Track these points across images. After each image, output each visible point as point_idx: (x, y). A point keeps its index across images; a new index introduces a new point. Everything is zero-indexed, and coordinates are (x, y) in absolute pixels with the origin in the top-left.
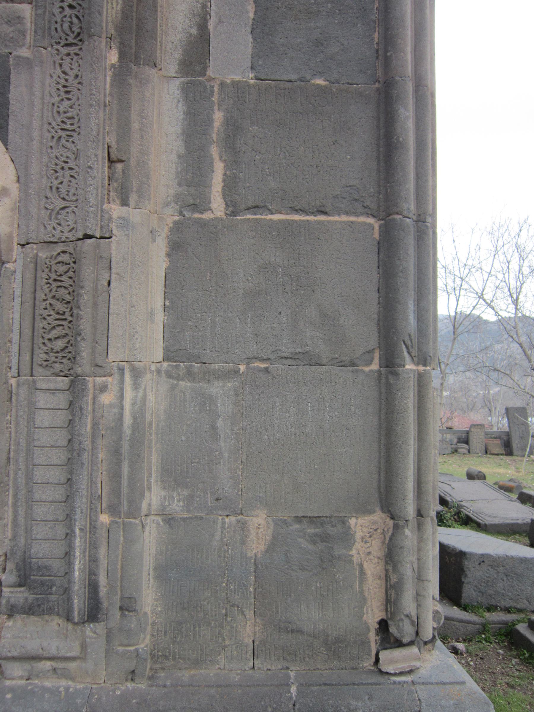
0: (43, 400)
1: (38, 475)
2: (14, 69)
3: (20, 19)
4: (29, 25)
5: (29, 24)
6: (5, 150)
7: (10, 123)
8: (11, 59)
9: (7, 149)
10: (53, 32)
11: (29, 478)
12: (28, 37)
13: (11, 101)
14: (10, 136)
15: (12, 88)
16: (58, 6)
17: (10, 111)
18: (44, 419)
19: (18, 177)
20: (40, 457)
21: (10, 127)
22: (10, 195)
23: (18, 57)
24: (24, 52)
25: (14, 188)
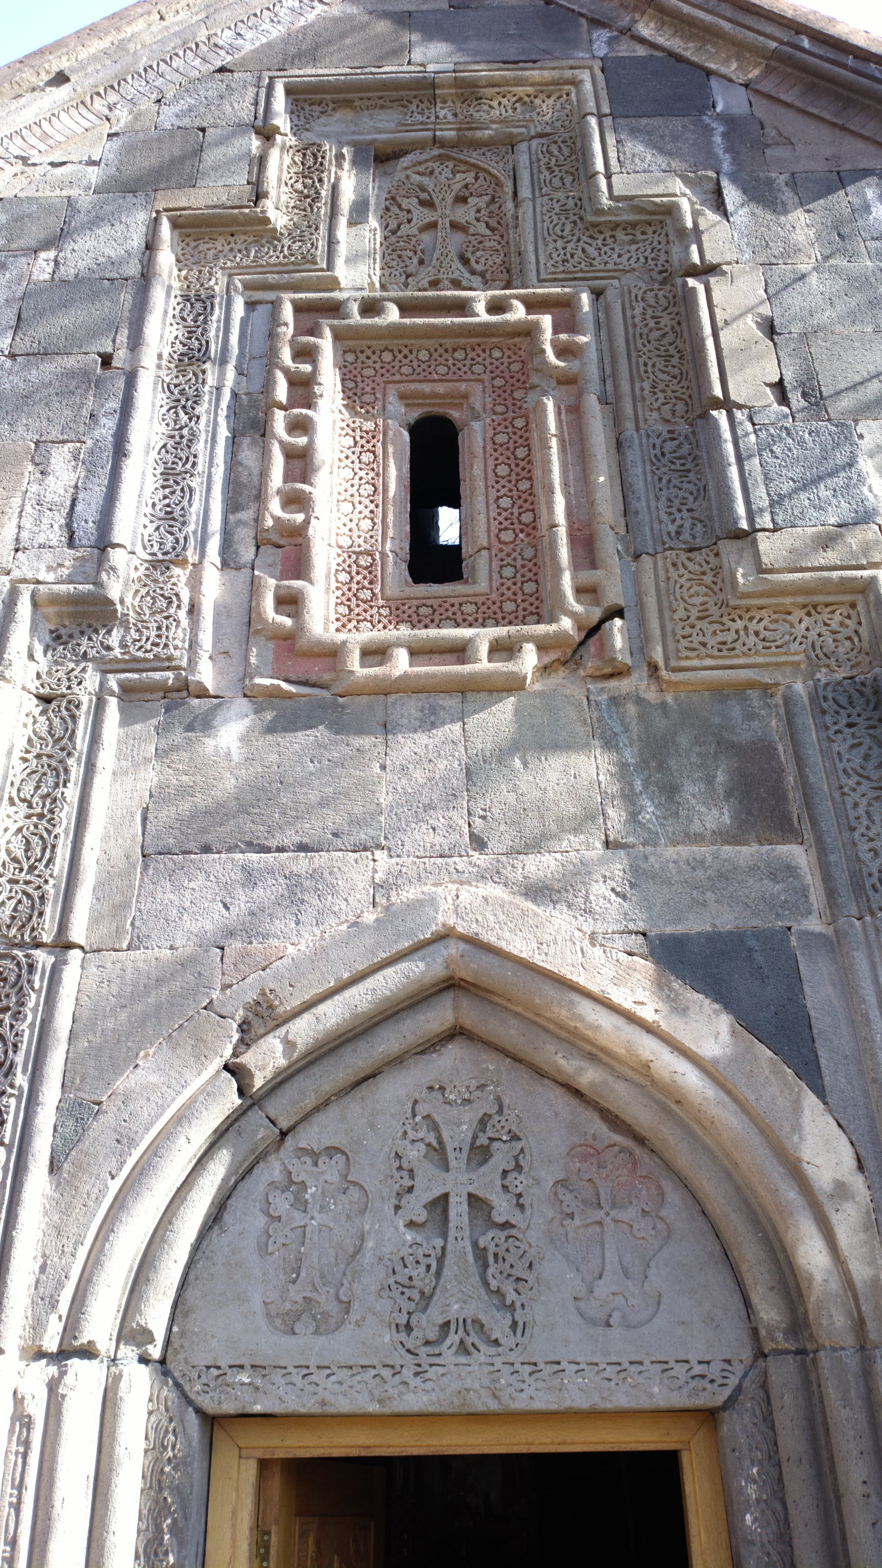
2: (803, 954)
3: (790, 870)
5: (809, 877)
6: (822, 1106)
7: (820, 1053)
8: (793, 938)
9: (825, 1103)
10: (871, 893)
12: (813, 898)
13: (812, 1013)
14: (827, 1080)
15: (807, 990)
16: (866, 847)
17: (815, 1031)
19: (859, 1160)
21: (823, 1062)
22: (853, 1197)
23: (805, 935)
24: (814, 925)
25: (858, 1183)
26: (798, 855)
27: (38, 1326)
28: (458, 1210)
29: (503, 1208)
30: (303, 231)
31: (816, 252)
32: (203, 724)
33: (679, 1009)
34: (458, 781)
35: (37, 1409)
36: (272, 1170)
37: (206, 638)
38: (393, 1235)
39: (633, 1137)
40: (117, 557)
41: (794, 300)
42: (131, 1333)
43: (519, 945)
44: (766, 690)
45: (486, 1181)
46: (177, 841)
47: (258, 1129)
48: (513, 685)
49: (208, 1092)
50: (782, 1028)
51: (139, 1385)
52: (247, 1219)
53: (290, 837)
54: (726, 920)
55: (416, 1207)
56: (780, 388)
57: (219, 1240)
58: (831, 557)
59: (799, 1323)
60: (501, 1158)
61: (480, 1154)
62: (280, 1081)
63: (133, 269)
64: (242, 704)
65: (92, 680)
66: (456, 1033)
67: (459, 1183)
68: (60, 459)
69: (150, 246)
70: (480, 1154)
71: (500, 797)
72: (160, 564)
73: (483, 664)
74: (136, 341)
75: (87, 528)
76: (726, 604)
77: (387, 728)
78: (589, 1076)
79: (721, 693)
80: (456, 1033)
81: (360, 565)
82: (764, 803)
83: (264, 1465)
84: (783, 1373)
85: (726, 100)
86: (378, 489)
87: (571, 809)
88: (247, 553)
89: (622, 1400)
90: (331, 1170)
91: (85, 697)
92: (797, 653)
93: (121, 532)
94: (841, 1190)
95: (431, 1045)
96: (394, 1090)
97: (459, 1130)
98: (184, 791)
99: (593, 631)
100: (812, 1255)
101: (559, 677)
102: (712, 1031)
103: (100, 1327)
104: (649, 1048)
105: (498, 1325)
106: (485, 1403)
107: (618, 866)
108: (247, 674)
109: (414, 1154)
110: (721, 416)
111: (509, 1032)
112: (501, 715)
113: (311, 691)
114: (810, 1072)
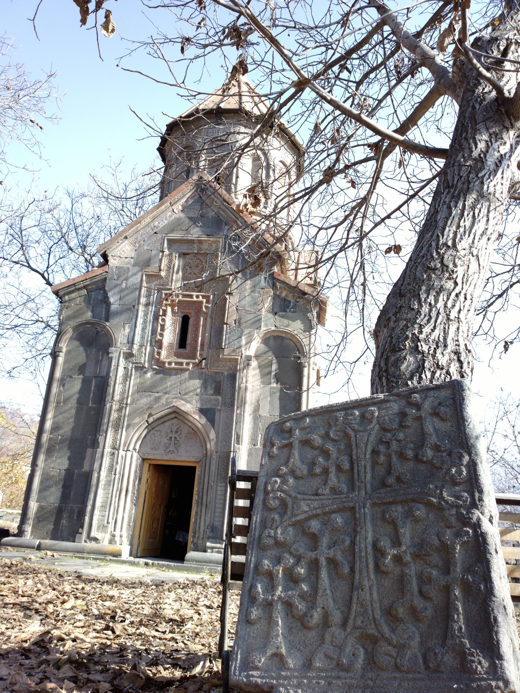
0: (219, 488)
1: (217, 505)
3: (218, 400)
4: (220, 401)
11: (215, 506)
18: (219, 493)
20: (217, 501)
24: (219, 408)
26: (220, 398)
27: (124, 448)
28: (173, 438)
29: (178, 439)
30: (168, 275)
31: (249, 291)
32: (146, 373)
33: (200, 417)
34: (179, 384)
35: (124, 456)
36: (152, 432)
37: (147, 359)
38: (165, 441)
39: (194, 432)
40: (135, 346)
41: (243, 303)
42: (135, 449)
43: (183, 408)
44: (222, 373)
45: (177, 435)
46: (142, 390)
47: (150, 428)
48: (188, 370)
49: (144, 424)
50: (212, 421)
51: (135, 455)
52: (148, 438)
53: (155, 390)
54: (209, 406)
55: (168, 438)
56: (235, 321)
57: (145, 440)
58: (234, 354)
59: (206, 454)
60: (179, 433)
61: (176, 432)
62: (152, 423)
63: (138, 287)
64: (151, 370)
65: (131, 365)
66: (175, 417)
67: (173, 435)
68: (127, 326)
69: (142, 280)
70: (176, 432)
71: (184, 386)
72: (141, 346)
73: (185, 366)
74: (139, 303)
75: (130, 340)
76: (218, 360)
77: (170, 375)
78: (190, 424)
79: (216, 373)
80: (175, 417)
81: (171, 345)
82: (218, 391)
83: (150, 465)
84: (204, 458)
86: (175, 330)
87: (192, 389)
88: (154, 344)
89: (188, 460)
90: (159, 433)
91: (130, 368)
92: (227, 368)
93: (136, 342)
94: (213, 439)
95: (172, 419)
96: (167, 424)
97: (174, 430)
98: (143, 383)
99: (201, 362)
100: (208, 446)
101: (196, 368)
102: (203, 420)
103: (131, 448)
104: (196, 422)
105: (176, 451)
106: (173, 459)
107: (198, 397)
108: (152, 365)
109: (169, 432)
110: (225, 326)
111: (181, 418)
112: (186, 374)
114: (213, 426)
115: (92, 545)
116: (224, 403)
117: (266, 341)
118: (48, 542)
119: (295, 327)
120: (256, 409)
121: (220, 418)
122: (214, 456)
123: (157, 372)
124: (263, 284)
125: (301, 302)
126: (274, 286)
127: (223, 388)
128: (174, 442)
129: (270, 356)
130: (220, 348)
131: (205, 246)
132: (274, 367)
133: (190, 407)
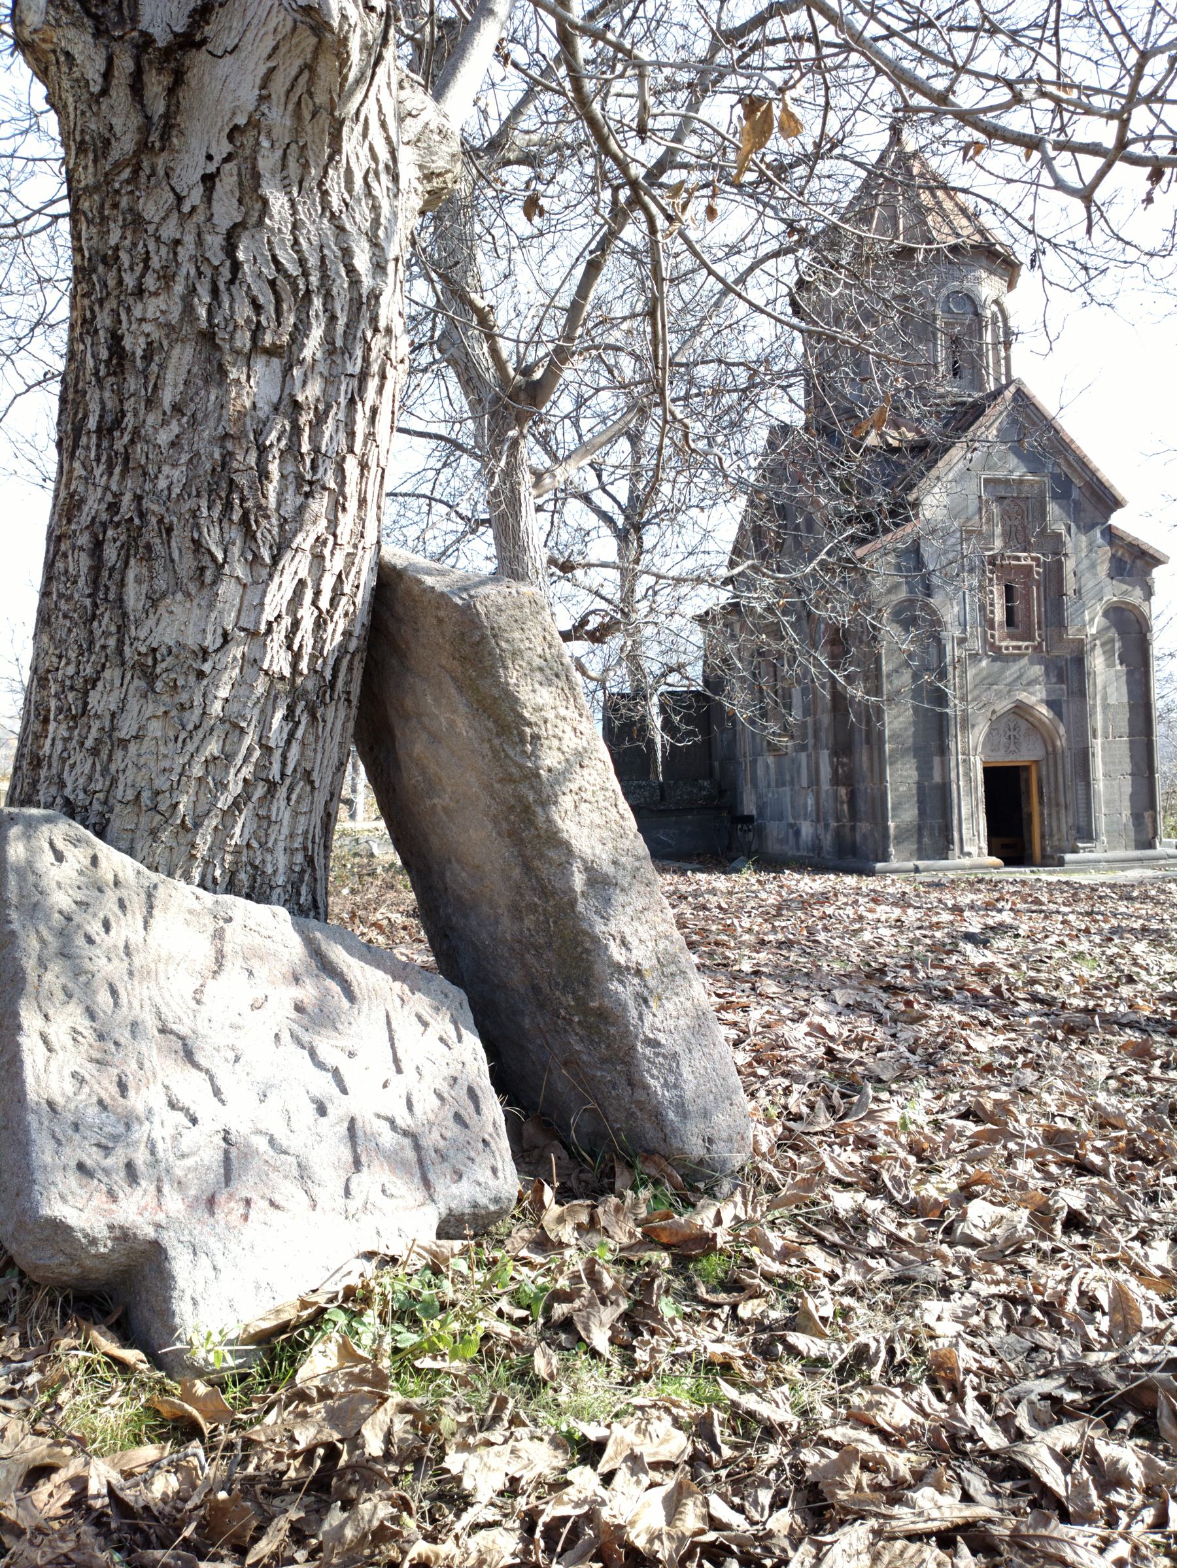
38: (1004, 740)
39: (1035, 727)
82: (1061, 679)
85: (1075, 494)
112: (1025, 660)
113: (998, 656)
115: (966, 861)
116: (1070, 693)
117: (1106, 614)
118: (921, 864)
119: (1135, 596)
120: (1105, 698)
121: (1069, 709)
122: (1068, 753)
123: (994, 660)
124: (1100, 541)
125: (1139, 563)
126: (1111, 543)
127: (1069, 672)
128: (1014, 741)
129: (1113, 633)
130: (1061, 625)
131: (1025, 488)
132: (1117, 645)
133: (1035, 698)
